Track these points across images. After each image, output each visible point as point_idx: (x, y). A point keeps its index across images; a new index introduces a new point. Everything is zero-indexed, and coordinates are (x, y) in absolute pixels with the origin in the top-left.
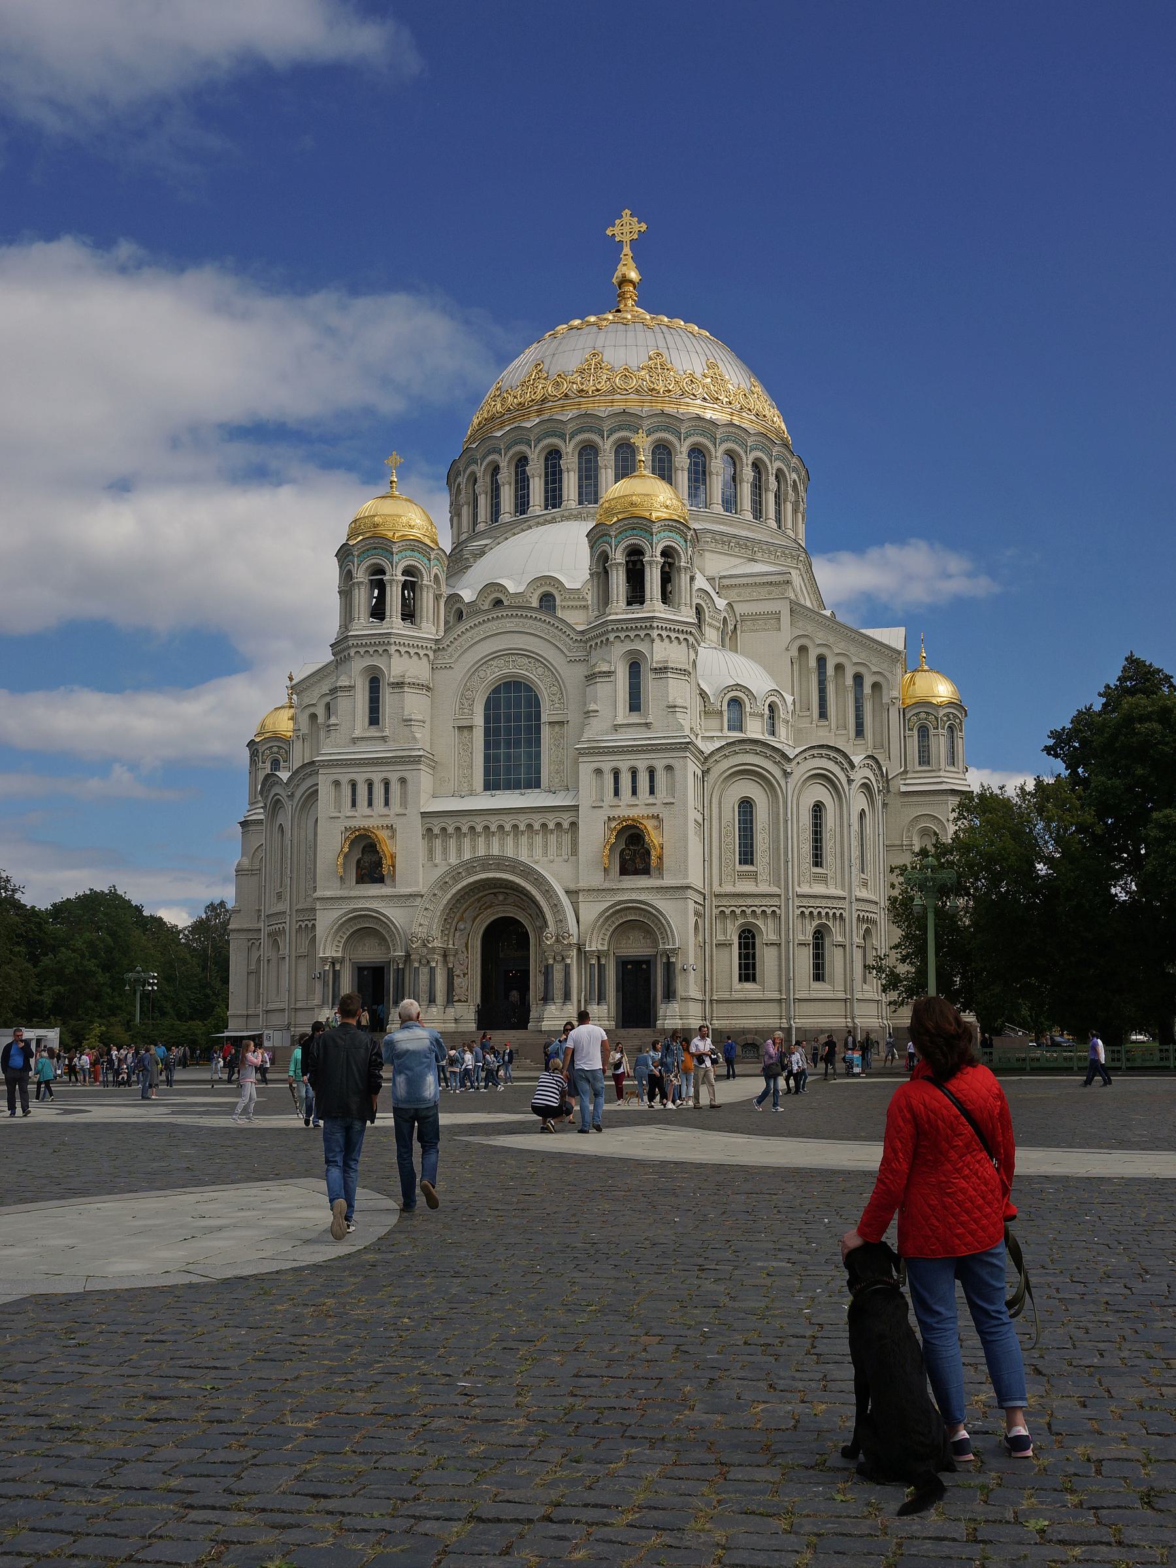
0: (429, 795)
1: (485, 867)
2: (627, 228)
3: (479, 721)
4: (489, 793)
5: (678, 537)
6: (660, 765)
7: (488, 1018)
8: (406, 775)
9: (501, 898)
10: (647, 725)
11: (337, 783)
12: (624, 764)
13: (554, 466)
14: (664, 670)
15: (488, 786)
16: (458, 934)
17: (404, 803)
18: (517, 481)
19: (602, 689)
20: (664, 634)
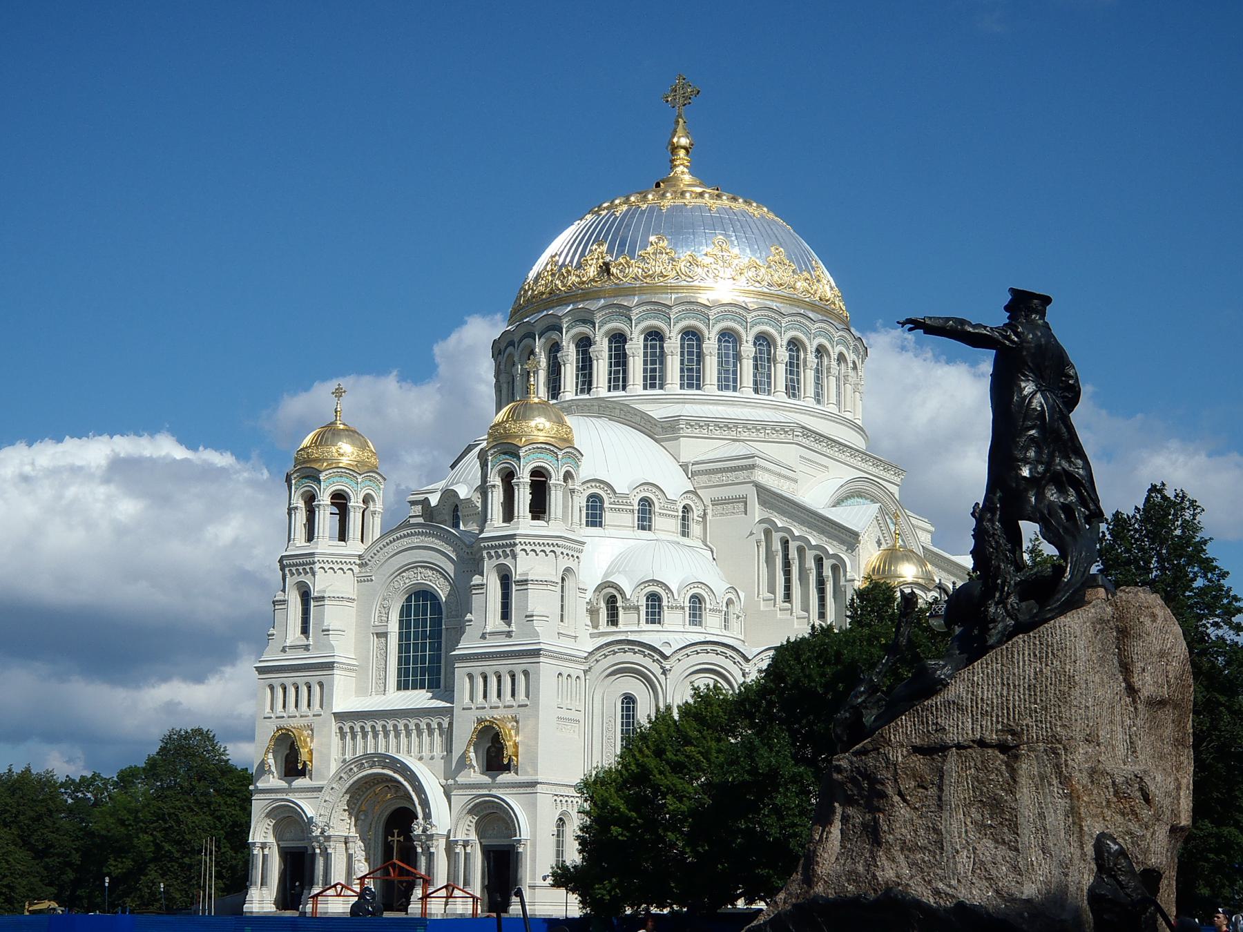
3: (394, 627)
5: (549, 457)
6: (518, 670)
10: (509, 634)
12: (490, 667)
14: (525, 582)
15: (399, 689)
16: (359, 822)
19: (476, 601)
20: (528, 548)
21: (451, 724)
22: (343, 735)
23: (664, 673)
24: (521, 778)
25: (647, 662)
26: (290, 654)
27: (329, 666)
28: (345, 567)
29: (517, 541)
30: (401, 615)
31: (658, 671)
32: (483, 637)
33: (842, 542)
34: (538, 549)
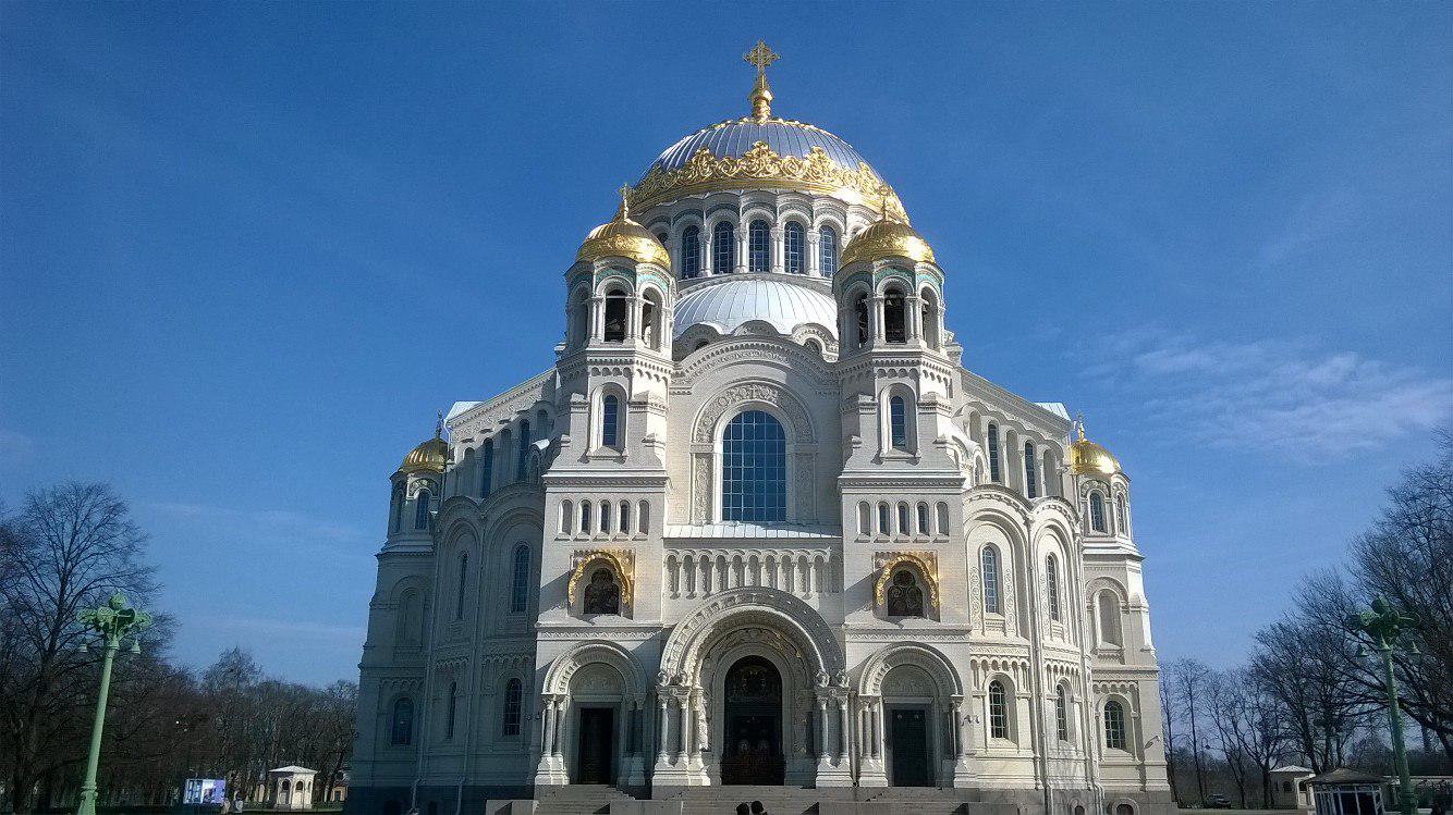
0: (677, 518)
1: (746, 599)
2: (760, 55)
3: (719, 448)
4: (727, 522)
6: (932, 501)
7: (733, 769)
8: (646, 497)
9: (753, 635)
10: (914, 461)
11: (568, 505)
12: (893, 497)
13: (724, 236)
17: (644, 529)
18: (684, 249)
19: (866, 421)
20: (929, 371)
21: (837, 560)
22: (672, 563)
23: (1028, 523)
24: (944, 624)
25: (1010, 511)
26: (593, 465)
27: (660, 482)
28: (661, 375)
29: (923, 360)
30: (726, 435)
31: (1021, 522)
32: (878, 460)
33: (1050, 430)
34: (936, 373)
